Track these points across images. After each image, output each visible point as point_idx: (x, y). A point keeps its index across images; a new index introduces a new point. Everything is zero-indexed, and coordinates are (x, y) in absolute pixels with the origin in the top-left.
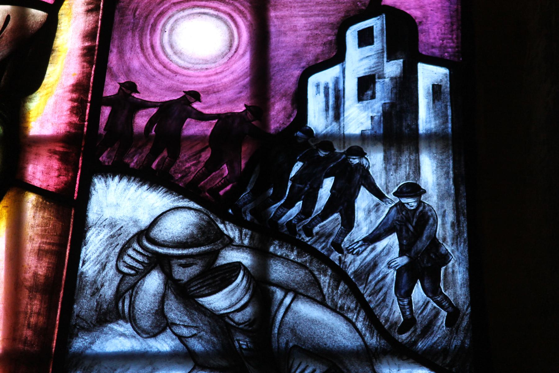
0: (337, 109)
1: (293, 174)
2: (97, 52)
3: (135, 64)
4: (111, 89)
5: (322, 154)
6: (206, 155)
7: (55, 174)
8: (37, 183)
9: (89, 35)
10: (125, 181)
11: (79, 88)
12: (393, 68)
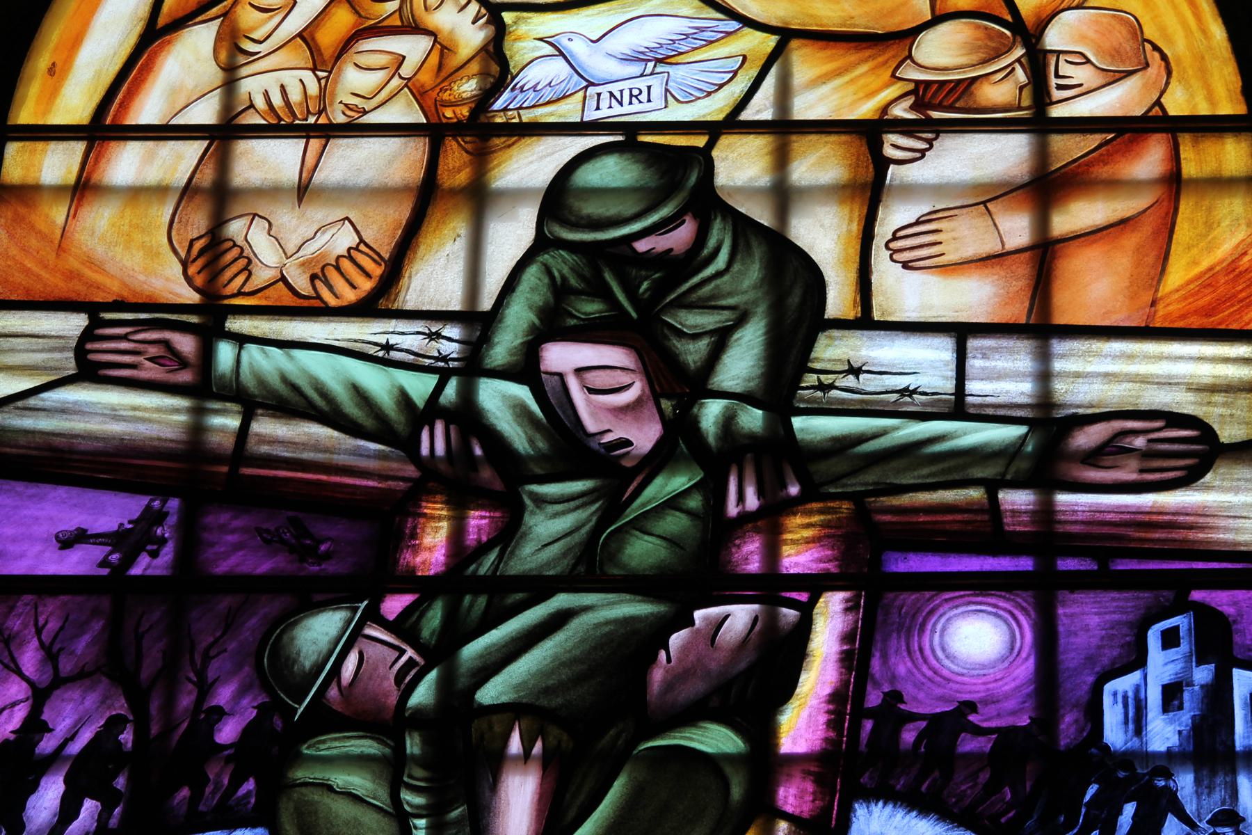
0: (1137, 719)
1: (1087, 798)
2: (856, 656)
3: (901, 670)
4: (873, 699)
5: (1121, 774)
6: (984, 777)
7: (809, 798)
8: (789, 809)
9: (847, 637)
10: (889, 807)
11: (837, 698)
12: (1203, 675)
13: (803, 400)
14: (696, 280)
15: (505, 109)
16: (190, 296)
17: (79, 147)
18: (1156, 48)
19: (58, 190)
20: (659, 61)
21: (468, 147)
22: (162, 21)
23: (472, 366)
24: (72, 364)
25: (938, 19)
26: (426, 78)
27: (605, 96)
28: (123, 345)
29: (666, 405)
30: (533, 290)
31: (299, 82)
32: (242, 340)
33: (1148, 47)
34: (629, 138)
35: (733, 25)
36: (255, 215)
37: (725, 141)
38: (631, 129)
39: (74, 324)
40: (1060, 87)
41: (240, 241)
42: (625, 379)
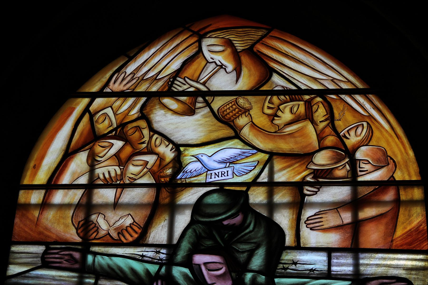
13: (278, 273)
14: (243, 234)
15: (181, 179)
16: (78, 239)
17: (43, 192)
18: (391, 158)
19: (36, 206)
20: (230, 163)
21: (169, 191)
22: (70, 151)
23: (170, 262)
24: (40, 262)
25: (321, 149)
26: (155, 168)
27: (213, 174)
28: (57, 256)
29: (233, 274)
30: (190, 237)
31: (115, 170)
32: (95, 254)
33: (389, 158)
34: (221, 188)
35: (255, 151)
36: (100, 213)
37: (252, 188)
38: (222, 185)
39: (40, 249)
40: (361, 171)
41: (95, 221)
42: (220, 266)
